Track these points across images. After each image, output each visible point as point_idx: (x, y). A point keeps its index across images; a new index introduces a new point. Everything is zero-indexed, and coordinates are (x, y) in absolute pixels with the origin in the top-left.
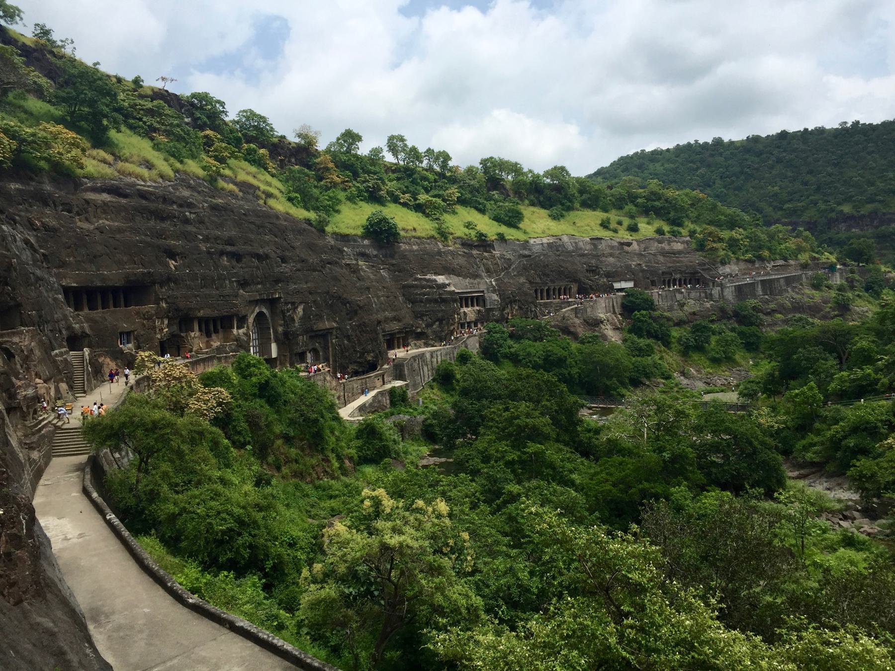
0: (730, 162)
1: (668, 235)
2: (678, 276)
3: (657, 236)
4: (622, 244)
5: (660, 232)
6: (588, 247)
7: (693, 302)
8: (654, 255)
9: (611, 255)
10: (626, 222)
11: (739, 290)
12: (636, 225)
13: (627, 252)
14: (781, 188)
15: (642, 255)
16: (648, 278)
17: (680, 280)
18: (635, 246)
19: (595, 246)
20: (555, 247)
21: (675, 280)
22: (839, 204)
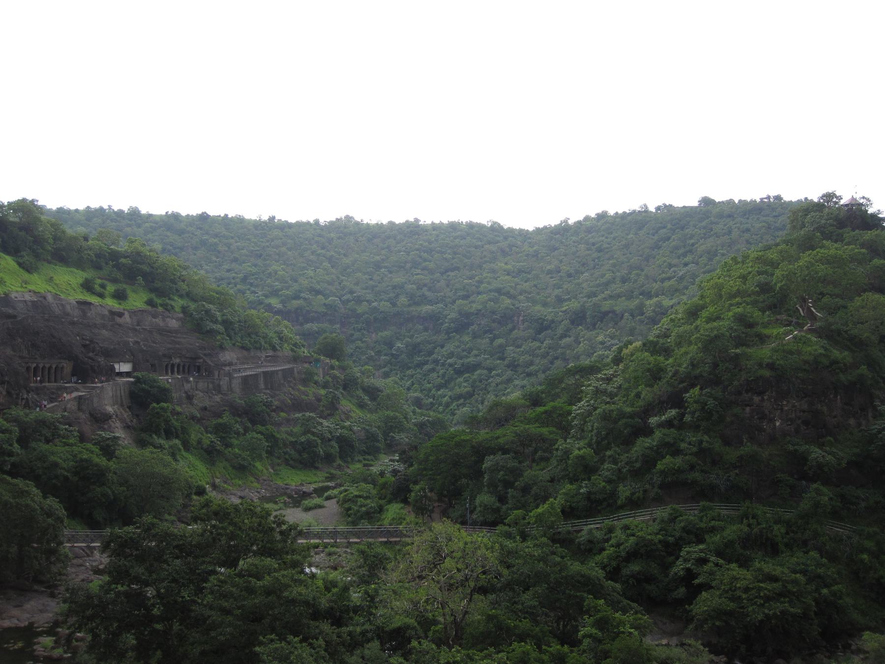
0: (150, 236)
1: (160, 309)
2: (178, 360)
3: (149, 308)
4: (113, 313)
5: (150, 303)
6: (77, 312)
7: (201, 394)
8: (150, 332)
9: (104, 326)
10: (111, 288)
11: (245, 379)
12: (124, 290)
13: (120, 325)
14: (207, 272)
15: (136, 330)
16: (147, 361)
17: (179, 365)
18: (127, 318)
19: (84, 312)
20: (39, 305)
21: (173, 366)
22: (266, 296)
